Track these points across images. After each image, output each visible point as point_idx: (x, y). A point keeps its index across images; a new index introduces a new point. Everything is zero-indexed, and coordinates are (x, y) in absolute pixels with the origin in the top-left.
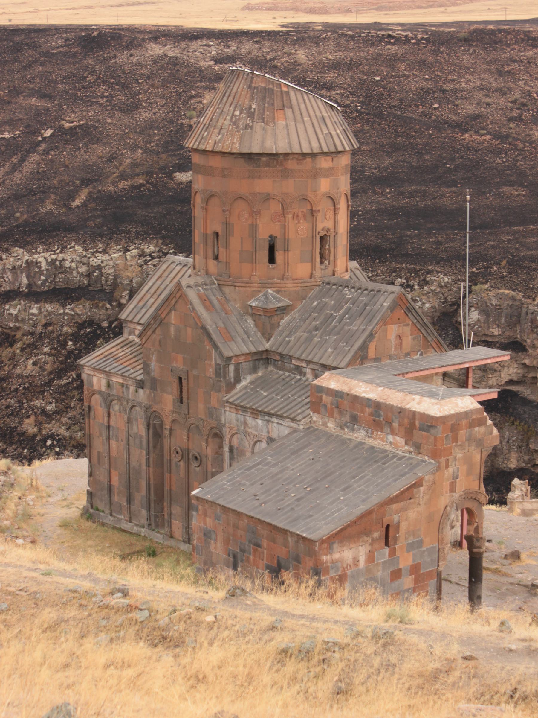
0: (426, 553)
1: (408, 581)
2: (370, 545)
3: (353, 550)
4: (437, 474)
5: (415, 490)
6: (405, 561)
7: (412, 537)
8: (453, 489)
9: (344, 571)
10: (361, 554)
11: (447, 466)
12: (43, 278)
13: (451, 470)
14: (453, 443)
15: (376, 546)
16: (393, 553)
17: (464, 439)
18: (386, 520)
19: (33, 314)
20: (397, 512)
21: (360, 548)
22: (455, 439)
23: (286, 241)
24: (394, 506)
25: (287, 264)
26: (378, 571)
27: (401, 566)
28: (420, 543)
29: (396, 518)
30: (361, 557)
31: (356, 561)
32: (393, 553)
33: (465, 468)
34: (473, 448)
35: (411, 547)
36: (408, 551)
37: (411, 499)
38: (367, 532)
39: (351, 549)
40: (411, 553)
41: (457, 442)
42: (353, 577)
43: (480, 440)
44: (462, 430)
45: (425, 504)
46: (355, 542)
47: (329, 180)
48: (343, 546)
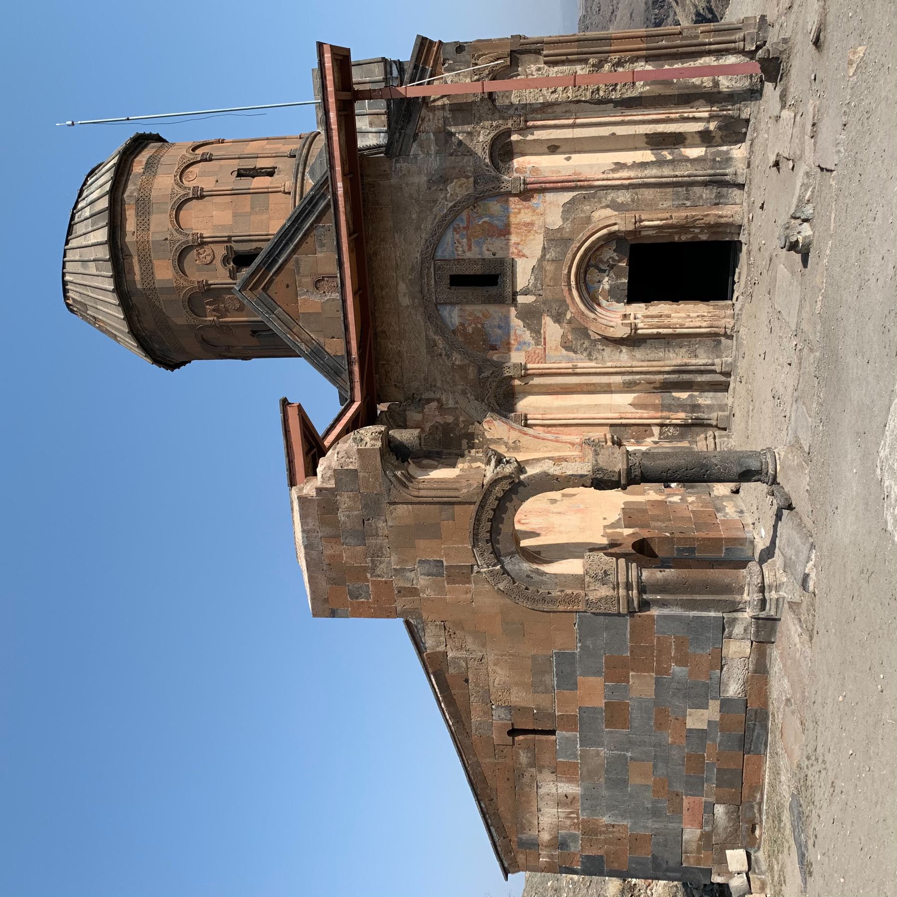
0: (589, 643)
1: (641, 686)
2: (541, 772)
3: (542, 804)
4: (425, 616)
5: (452, 671)
6: (593, 691)
7: (547, 678)
8: (462, 574)
9: (578, 824)
10: (554, 791)
11: (413, 592)
13: (422, 581)
14: (367, 581)
15: (546, 758)
16: (569, 722)
17: (360, 548)
18: (498, 737)
20: (488, 713)
21: (542, 791)
22: (359, 573)
24: (475, 718)
26: (598, 754)
27: (600, 703)
28: (565, 659)
29: (500, 717)
30: (560, 791)
31: (565, 801)
32: (569, 722)
33: (421, 543)
34: (381, 524)
35: (567, 681)
36: (574, 686)
37: (467, 681)
38: (516, 777)
39: (539, 810)
40: (580, 679)
41: (365, 569)
42: (593, 809)
43: (366, 506)
44: (341, 556)
45: (484, 645)
46: (528, 802)
47: (156, 263)
48: (530, 823)
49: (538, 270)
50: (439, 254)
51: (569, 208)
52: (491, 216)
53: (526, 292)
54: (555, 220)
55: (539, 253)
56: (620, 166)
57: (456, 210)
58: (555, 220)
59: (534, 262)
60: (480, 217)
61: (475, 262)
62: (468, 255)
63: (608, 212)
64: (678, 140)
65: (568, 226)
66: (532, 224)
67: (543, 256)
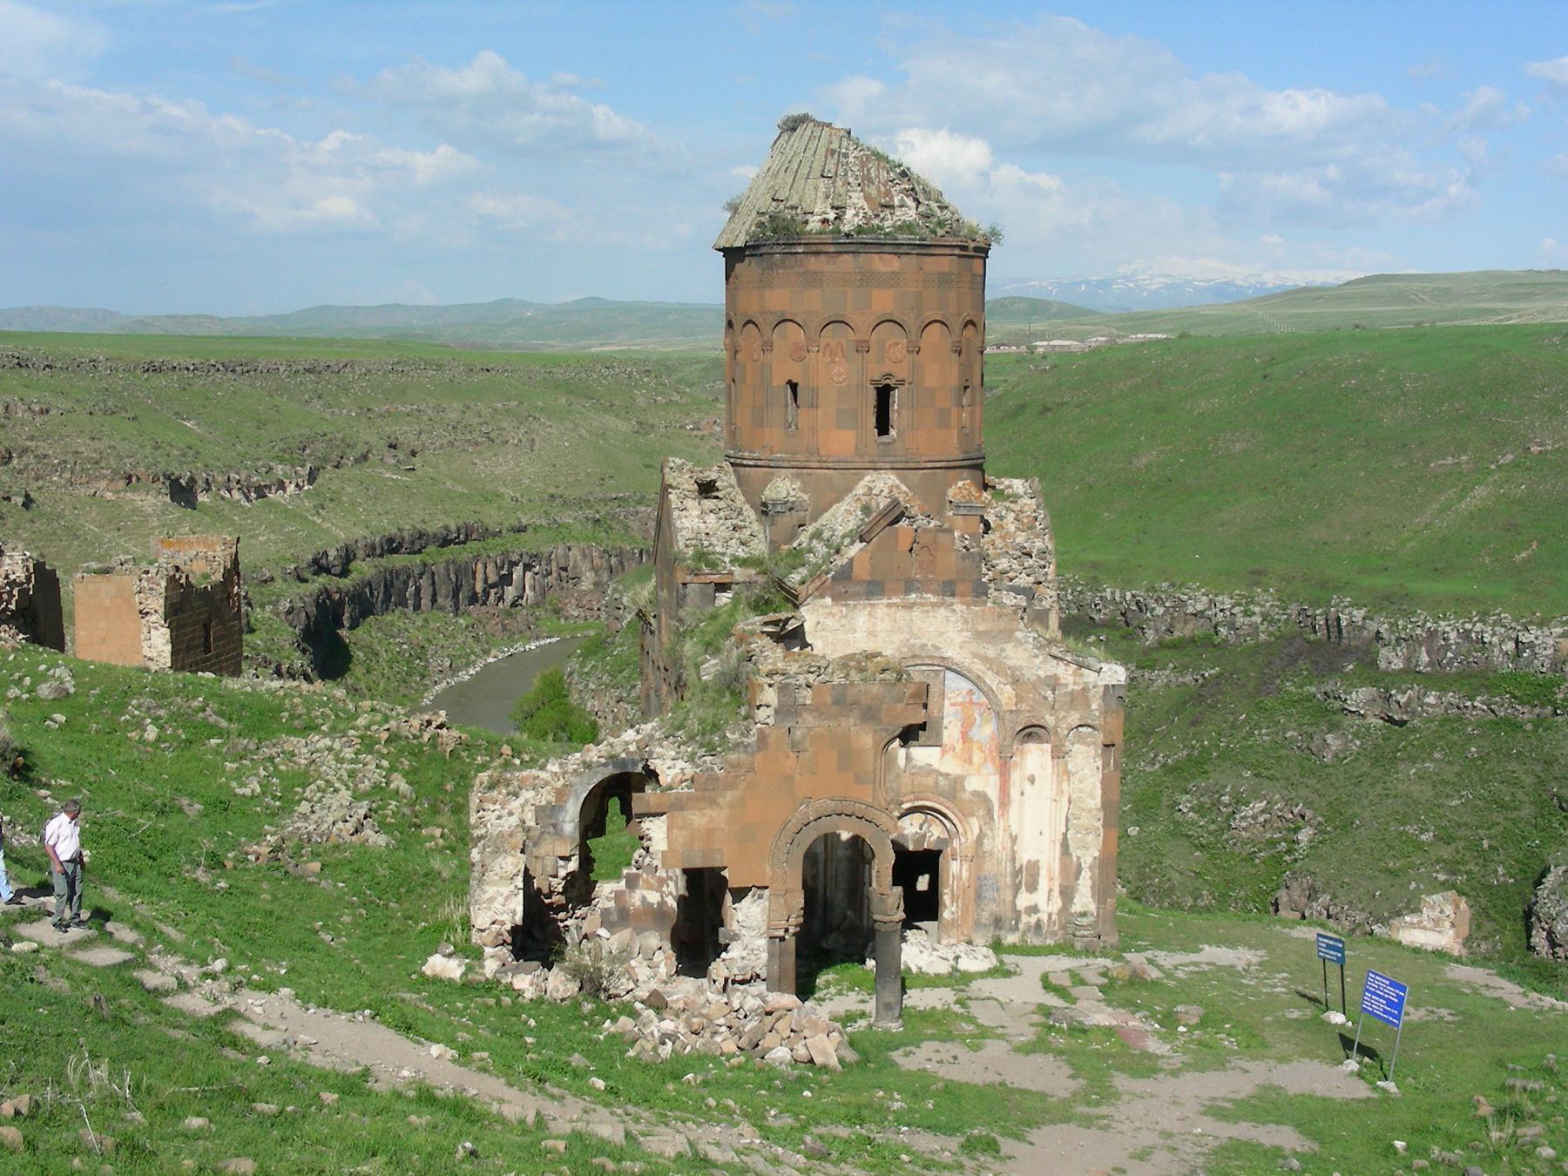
12: (1449, 654)
19: (1429, 705)
23: (815, 392)
25: (814, 430)
34: (852, 721)
43: (870, 708)
49: (929, 770)
50: (949, 674)
51: (982, 797)
52: (981, 726)
53: (908, 758)
54: (973, 784)
55: (943, 770)
56: (1014, 840)
57: (988, 693)
58: (973, 784)
59: (936, 766)
60: (981, 715)
61: (941, 709)
62: (947, 703)
63: (976, 831)
64: (1032, 887)
65: (966, 796)
66: (971, 763)
67: (941, 774)
